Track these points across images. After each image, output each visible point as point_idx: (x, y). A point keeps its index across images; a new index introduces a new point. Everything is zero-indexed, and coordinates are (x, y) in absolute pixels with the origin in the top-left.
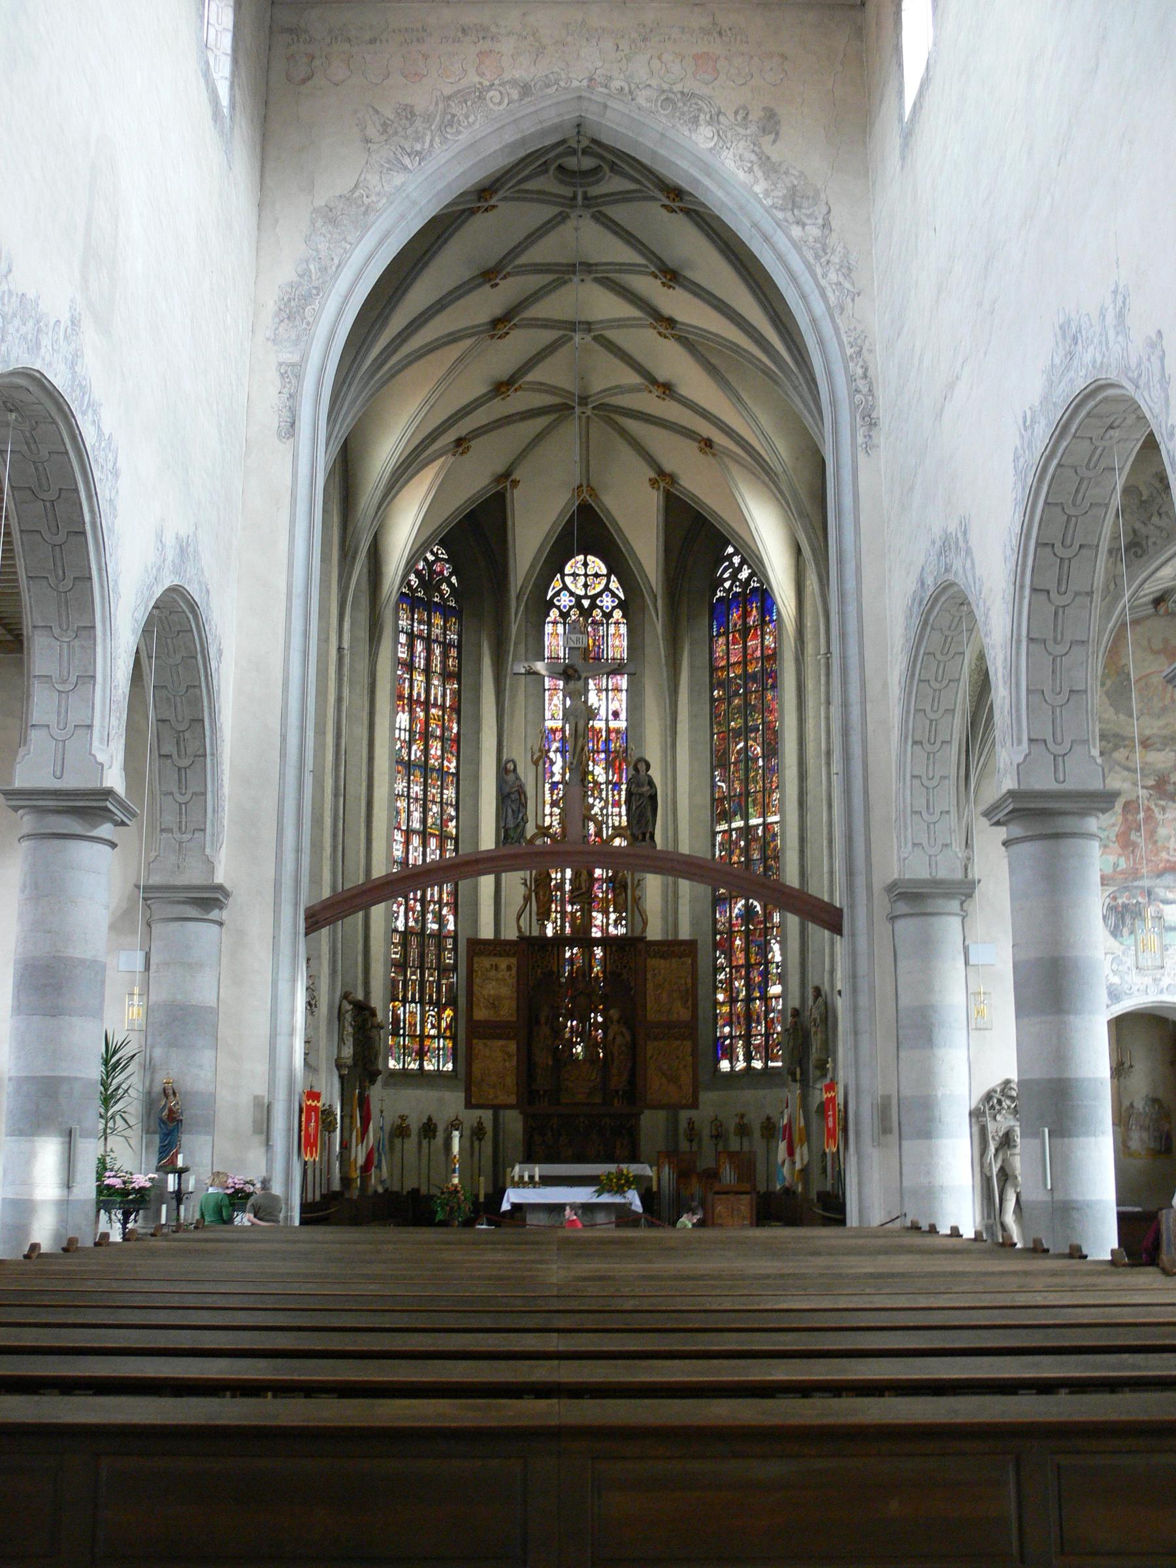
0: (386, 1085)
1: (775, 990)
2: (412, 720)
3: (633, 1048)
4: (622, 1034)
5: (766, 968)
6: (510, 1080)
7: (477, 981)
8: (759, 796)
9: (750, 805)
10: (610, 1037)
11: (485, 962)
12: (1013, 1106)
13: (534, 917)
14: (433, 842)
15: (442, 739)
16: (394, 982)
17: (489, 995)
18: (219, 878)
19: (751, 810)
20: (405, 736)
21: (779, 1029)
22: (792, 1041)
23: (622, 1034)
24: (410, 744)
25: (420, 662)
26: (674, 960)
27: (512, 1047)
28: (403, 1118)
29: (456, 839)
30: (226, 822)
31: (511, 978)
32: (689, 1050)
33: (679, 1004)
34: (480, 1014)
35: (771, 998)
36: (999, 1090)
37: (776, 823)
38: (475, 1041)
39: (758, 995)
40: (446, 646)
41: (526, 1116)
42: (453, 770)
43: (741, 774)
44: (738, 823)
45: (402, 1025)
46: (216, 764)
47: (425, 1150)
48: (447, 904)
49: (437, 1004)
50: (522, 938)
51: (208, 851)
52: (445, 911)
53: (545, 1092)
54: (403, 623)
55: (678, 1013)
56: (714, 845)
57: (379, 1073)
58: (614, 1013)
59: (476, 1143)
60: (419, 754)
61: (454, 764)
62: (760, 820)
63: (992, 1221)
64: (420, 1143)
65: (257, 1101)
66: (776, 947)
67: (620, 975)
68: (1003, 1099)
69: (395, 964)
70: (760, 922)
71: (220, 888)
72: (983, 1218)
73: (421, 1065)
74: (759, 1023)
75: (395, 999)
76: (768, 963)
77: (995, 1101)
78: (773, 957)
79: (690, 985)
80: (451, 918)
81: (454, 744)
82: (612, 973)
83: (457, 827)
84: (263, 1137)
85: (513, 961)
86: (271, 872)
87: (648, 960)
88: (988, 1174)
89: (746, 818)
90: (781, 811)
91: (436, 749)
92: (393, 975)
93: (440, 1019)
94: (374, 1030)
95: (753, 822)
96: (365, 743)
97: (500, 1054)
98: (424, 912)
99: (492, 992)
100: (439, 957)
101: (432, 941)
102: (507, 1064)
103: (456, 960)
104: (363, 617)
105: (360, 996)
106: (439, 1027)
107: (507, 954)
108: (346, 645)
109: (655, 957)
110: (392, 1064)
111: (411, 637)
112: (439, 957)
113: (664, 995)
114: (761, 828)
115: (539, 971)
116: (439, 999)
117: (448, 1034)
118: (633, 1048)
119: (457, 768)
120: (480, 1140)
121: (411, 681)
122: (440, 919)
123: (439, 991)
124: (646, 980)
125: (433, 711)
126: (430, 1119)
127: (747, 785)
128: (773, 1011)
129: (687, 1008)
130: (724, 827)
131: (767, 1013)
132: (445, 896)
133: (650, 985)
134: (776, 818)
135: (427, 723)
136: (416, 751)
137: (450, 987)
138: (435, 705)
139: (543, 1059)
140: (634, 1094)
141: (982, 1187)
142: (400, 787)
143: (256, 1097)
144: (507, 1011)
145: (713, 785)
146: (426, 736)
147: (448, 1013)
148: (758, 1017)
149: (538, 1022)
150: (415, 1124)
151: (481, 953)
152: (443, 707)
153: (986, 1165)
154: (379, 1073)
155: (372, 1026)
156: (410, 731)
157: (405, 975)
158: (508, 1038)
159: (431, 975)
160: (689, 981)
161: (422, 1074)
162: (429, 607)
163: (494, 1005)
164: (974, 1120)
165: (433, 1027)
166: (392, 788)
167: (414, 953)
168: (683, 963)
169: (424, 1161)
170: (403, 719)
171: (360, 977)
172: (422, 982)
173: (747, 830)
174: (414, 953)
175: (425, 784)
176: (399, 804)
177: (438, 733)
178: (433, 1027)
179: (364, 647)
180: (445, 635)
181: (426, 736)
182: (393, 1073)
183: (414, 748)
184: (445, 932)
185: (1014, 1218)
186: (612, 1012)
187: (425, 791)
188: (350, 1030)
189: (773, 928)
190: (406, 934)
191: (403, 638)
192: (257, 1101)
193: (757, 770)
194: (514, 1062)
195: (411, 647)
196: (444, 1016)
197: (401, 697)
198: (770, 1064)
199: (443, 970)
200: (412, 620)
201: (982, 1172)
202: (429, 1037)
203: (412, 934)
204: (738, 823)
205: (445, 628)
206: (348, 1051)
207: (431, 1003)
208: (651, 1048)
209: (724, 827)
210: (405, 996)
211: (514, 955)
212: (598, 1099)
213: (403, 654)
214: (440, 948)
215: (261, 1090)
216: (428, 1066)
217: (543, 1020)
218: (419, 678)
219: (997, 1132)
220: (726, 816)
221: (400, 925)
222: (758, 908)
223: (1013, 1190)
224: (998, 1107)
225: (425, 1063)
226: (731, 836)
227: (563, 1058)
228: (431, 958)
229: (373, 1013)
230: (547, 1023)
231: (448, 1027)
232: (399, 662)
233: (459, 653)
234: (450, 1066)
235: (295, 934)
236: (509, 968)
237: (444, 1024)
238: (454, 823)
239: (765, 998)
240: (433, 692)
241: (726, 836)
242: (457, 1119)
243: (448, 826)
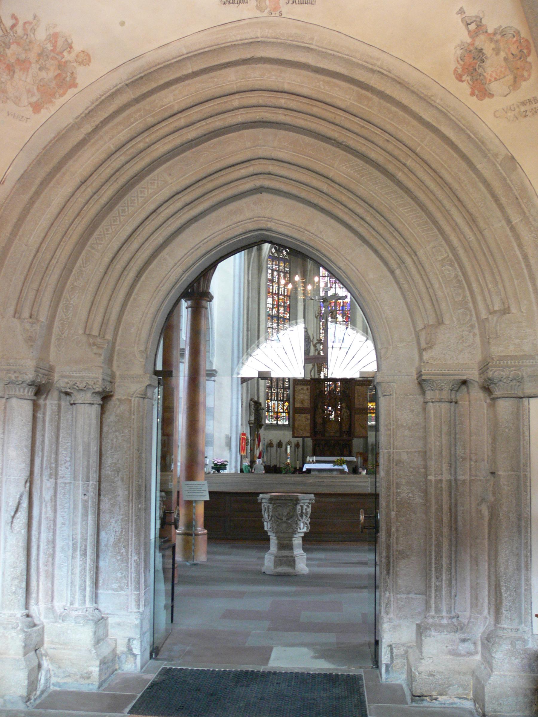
0: (265, 429)
2: (273, 300)
3: (350, 417)
6: (308, 428)
7: (296, 394)
10: (343, 413)
11: (300, 387)
13: (316, 372)
15: (284, 306)
16: (268, 393)
18: (214, 368)
20: (271, 306)
24: (272, 309)
25: (276, 280)
27: (309, 416)
28: (271, 441)
30: (215, 349)
31: (308, 393)
34: (298, 405)
40: (285, 273)
41: (313, 440)
42: (288, 318)
46: (212, 331)
47: (279, 452)
49: (283, 401)
50: (312, 379)
51: (211, 359)
54: (270, 266)
57: (262, 425)
59: (296, 449)
60: (276, 312)
61: (288, 315)
64: (277, 451)
65: (227, 436)
67: (346, 391)
69: (268, 387)
71: (215, 371)
73: (277, 422)
75: (268, 399)
81: (288, 308)
82: (343, 391)
84: (228, 447)
85: (309, 387)
86: (230, 365)
91: (282, 310)
93: (284, 406)
96: (257, 310)
99: (302, 398)
100: (283, 384)
103: (289, 385)
104: (256, 265)
105: (256, 399)
106: (283, 409)
107: (307, 385)
108: (250, 279)
109: (358, 385)
110: (267, 422)
111: (273, 270)
112: (283, 384)
113: (361, 399)
116: (283, 399)
118: (350, 417)
119: (289, 317)
120: (298, 448)
121: (273, 286)
123: (283, 396)
125: (280, 297)
126: (280, 441)
133: (356, 395)
135: (278, 301)
136: (275, 312)
137: (287, 395)
138: (281, 295)
139: (319, 421)
140: (350, 433)
142: (269, 324)
143: (226, 435)
144: (307, 404)
146: (278, 306)
147: (287, 404)
150: (275, 443)
151: (298, 385)
152: (284, 295)
154: (262, 425)
156: (273, 304)
159: (280, 391)
162: (279, 259)
163: (302, 402)
165: (281, 409)
166: (266, 325)
169: (278, 456)
170: (270, 300)
171: (256, 392)
172: (277, 393)
175: (278, 323)
176: (269, 330)
177: (282, 304)
178: (281, 409)
179: (256, 276)
180: (284, 269)
181: (278, 306)
183: (274, 310)
186: (343, 404)
187: (278, 325)
188: (253, 411)
191: (270, 271)
192: (227, 436)
194: (309, 422)
195: (272, 274)
196: (285, 405)
197: (269, 292)
199: (285, 389)
200: (273, 264)
202: (280, 412)
205: (284, 267)
206: (253, 418)
207: (280, 400)
208: (357, 417)
210: (271, 398)
211: (309, 385)
212: (338, 434)
213: (269, 276)
215: (228, 433)
216: (279, 423)
217: (319, 407)
218: (275, 285)
227: (326, 420)
229: (260, 404)
231: (287, 409)
232: (268, 280)
233: (290, 275)
234: (287, 423)
235: (238, 384)
236: (307, 389)
237: (285, 408)
240: (280, 290)
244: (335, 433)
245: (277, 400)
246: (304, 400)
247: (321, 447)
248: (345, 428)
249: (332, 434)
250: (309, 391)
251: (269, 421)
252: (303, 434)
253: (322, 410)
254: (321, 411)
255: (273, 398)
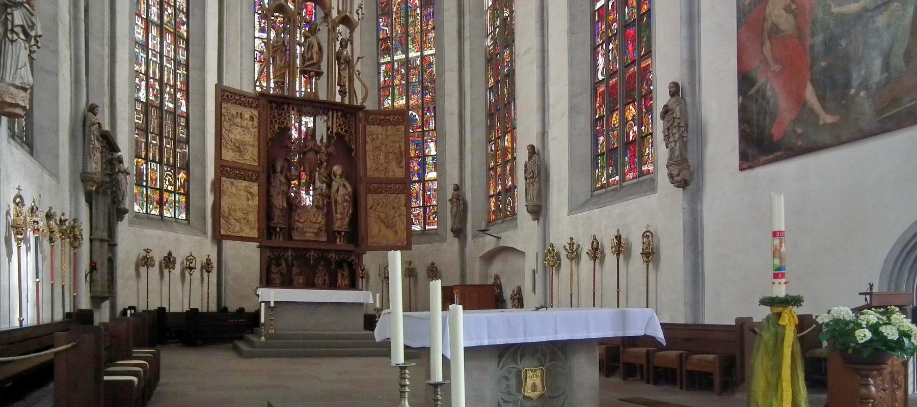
0: (131, 223)
1: (432, 175)
4: (344, 185)
5: (424, 159)
6: (253, 217)
8: (418, 37)
9: (410, 42)
14: (169, 38)
16: (137, 141)
17: (236, 140)
19: (410, 46)
21: (435, 203)
22: (455, 207)
23: (344, 185)
26: (389, 127)
27: (255, 188)
28: (147, 251)
29: (187, 41)
32: (404, 202)
33: (394, 164)
35: (427, 181)
37: (432, 55)
38: (223, 179)
39: (417, 179)
43: (403, 20)
44: (399, 56)
45: (145, 178)
48: (180, 90)
52: (179, 95)
53: (281, 229)
55: (394, 171)
56: (379, 73)
58: (337, 169)
62: (419, 54)
66: (432, 145)
69: (137, 127)
70: (419, 127)
74: (417, 198)
76: (424, 156)
78: (430, 151)
79: (403, 149)
80: (184, 102)
83: (188, 31)
87: (367, 127)
89: (406, 51)
90: (439, 44)
92: (136, 136)
94: (121, 174)
95: (412, 54)
97: (244, 193)
98: (162, 92)
101: (169, 116)
102: (250, 202)
109: (373, 124)
110: (137, 208)
113: (382, 156)
114: (419, 59)
115: (277, 126)
117: (182, 191)
122: (175, 100)
124: (365, 143)
126: (170, 254)
127: (407, 28)
128: (430, 190)
129: (402, 168)
130: (388, 59)
131: (424, 191)
132: (178, 83)
133: (369, 147)
134: (433, 52)
139: (279, 202)
144: (251, 157)
145: (378, 29)
148: (417, 193)
149: (275, 172)
150: (158, 256)
154: (126, 211)
155: (119, 171)
157: (147, 138)
158: (251, 180)
160: (403, 145)
161: (162, 219)
167: (154, 123)
168: (397, 130)
173: (407, 62)
174: (154, 123)
182: (137, 215)
184: (178, 112)
189: (429, 131)
190: (147, 105)
193: (415, 17)
194: (256, 202)
198: (427, 227)
203: (153, 106)
204: (399, 56)
209: (388, 59)
210: (147, 155)
212: (324, 238)
214: (175, 124)
217: (279, 169)
220: (388, 51)
221: (142, 96)
222: (417, 117)
225: (165, 211)
226: (393, 65)
227: (293, 205)
228: (168, 130)
230: (282, 172)
238: (185, 27)
239: (422, 180)
241: (389, 66)
242: (191, 255)
243: (180, 29)
244: (317, 234)
245: (160, 162)
246: (243, 143)
247: (284, 265)
248: (341, 222)
249: (310, 236)
250: (256, 124)
251: (141, 206)
252: (241, 230)
253: (286, 177)
254: (283, 179)
255: (151, 155)
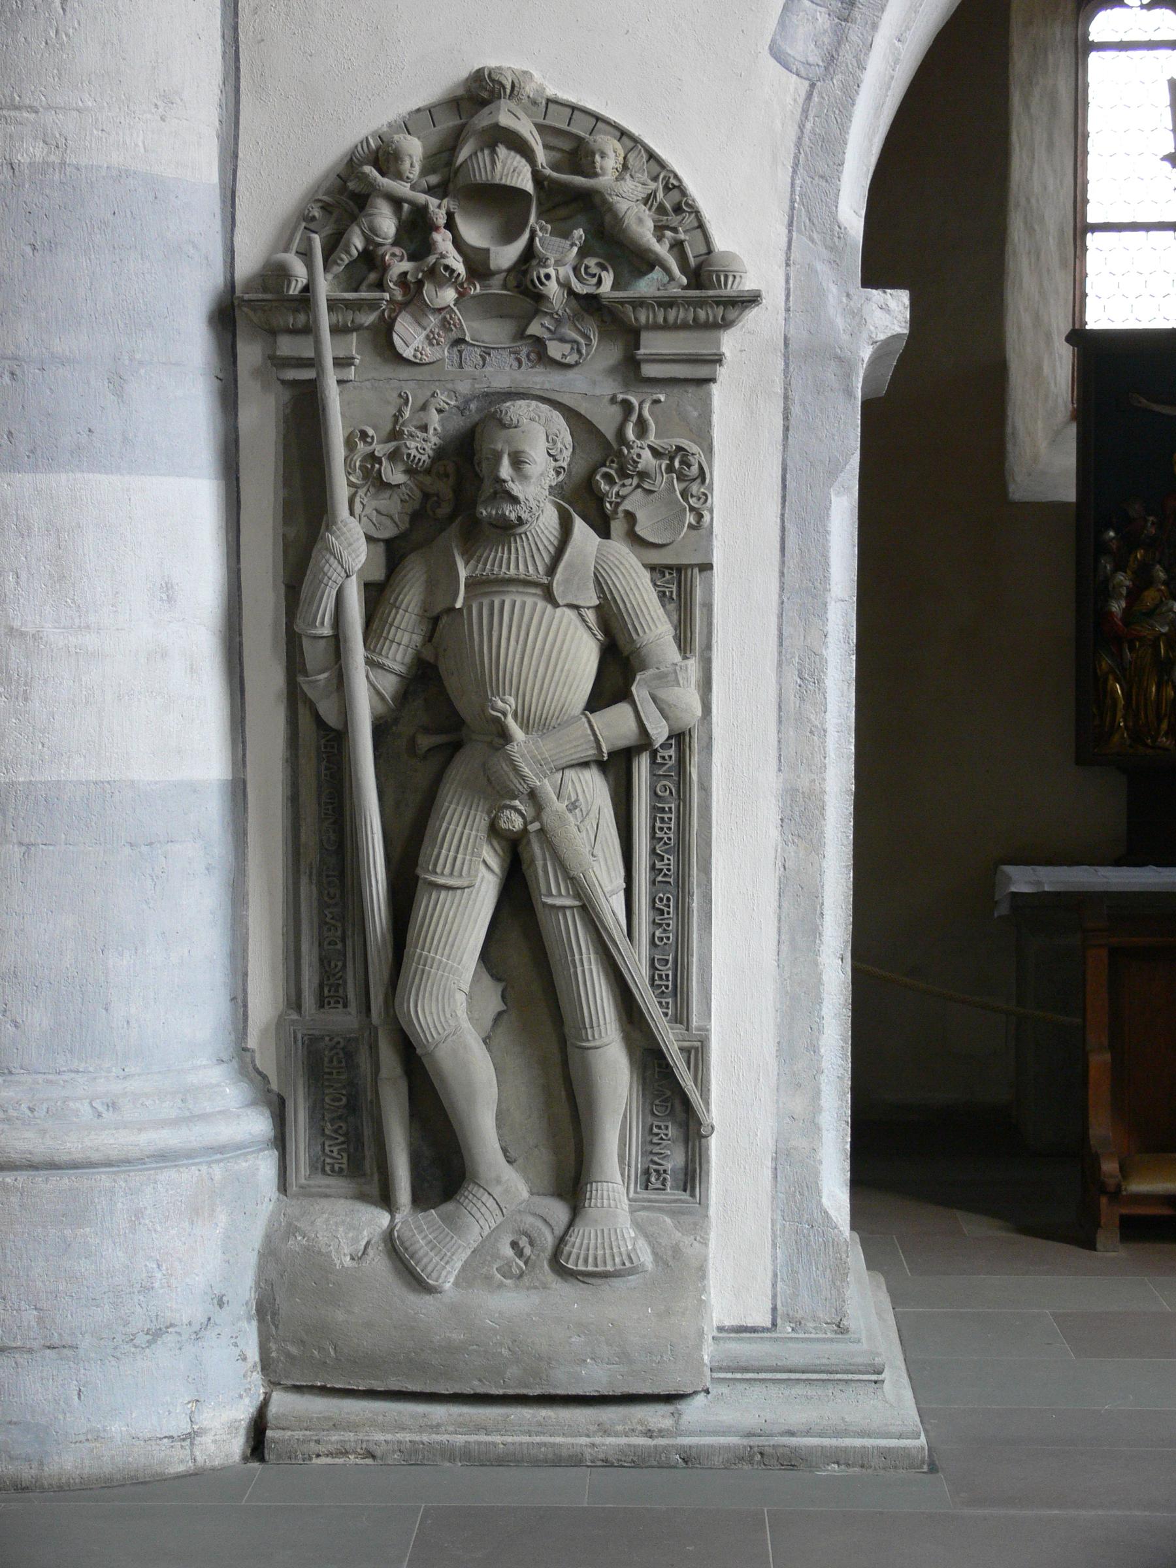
12: (506, 256)
36: (414, 149)
63: (344, 1020)
68: (438, 210)
72: (295, 1003)
77: (387, 224)
88: (328, 711)
141: (294, 799)
153: (314, 654)
164: (250, 353)
185: (492, 1003)
201: (294, 696)
219: (395, 435)
223: (481, 821)
224: (401, 266)
